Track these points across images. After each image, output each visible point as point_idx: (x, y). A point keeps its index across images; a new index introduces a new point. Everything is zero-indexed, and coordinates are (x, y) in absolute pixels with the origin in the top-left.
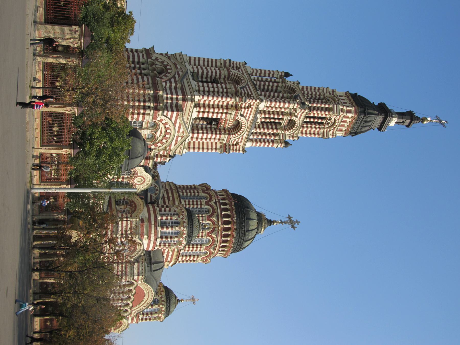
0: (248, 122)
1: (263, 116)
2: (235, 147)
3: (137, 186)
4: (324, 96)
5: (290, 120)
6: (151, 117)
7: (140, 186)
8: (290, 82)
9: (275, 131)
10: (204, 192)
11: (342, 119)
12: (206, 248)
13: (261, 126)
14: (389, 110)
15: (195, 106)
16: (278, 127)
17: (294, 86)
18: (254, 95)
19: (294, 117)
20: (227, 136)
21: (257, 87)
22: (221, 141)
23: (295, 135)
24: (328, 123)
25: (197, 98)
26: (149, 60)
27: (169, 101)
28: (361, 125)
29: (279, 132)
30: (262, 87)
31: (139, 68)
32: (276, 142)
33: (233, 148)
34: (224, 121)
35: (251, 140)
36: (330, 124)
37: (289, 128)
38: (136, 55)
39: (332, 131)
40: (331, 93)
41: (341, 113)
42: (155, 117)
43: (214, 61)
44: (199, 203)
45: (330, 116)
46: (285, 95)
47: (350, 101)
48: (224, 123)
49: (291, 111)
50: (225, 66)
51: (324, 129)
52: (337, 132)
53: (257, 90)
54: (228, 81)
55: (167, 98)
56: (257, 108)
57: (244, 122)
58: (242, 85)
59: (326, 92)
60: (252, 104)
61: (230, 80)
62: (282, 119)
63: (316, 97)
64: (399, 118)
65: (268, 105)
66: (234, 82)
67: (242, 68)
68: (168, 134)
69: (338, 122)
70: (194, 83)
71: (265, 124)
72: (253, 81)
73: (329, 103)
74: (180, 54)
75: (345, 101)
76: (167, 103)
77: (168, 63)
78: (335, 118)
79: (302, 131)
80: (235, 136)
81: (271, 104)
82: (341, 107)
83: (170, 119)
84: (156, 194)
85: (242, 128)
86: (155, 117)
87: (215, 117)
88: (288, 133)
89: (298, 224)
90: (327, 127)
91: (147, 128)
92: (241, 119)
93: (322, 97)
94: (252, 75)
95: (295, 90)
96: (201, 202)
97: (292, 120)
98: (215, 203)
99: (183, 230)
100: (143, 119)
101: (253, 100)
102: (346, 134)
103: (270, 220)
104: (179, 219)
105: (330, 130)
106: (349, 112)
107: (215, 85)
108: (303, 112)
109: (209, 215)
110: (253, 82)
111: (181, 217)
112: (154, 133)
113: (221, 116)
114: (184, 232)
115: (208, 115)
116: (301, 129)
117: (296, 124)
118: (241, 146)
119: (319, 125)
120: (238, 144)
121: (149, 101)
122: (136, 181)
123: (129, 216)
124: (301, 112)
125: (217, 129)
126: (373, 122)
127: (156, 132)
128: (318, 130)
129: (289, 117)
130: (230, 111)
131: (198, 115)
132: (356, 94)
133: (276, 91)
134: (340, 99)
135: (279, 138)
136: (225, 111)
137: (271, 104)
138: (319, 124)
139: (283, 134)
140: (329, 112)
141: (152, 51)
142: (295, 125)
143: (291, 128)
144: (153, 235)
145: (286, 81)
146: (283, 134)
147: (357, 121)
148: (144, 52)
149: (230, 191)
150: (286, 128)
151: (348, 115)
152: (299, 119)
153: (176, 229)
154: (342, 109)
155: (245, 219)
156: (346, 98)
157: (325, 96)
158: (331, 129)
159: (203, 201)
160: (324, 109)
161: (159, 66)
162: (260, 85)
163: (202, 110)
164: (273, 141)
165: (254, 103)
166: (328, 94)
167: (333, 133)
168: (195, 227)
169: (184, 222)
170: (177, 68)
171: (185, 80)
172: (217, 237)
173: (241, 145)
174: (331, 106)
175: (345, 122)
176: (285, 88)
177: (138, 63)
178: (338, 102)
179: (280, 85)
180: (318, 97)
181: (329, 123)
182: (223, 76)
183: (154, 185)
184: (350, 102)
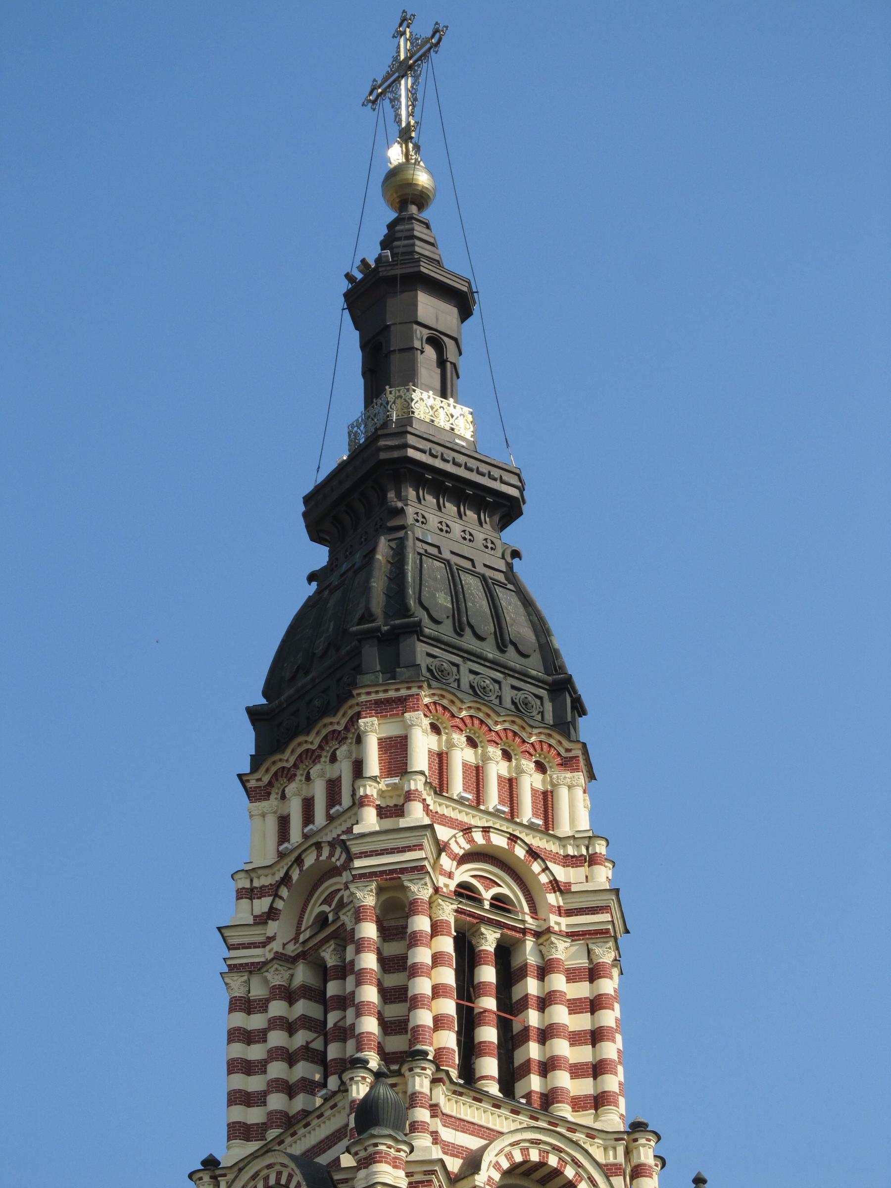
4: (293, 960)
11: (460, 801)
14: (357, 453)
23: (621, 1159)
24: (500, 903)
28: (489, 650)
36: (505, 890)
39: (561, 873)
40: (262, 905)
41: (416, 815)
45: (445, 897)
47: (312, 756)
51: (549, 930)
52: (564, 828)
59: (264, 945)
63: (306, 1022)
64: (410, 378)
69: (486, 830)
73: (346, 918)
75: (319, 791)
78: (453, 857)
79: (578, 1104)
82: (370, 820)
90: (534, 911)
93: (302, 975)
102: (567, 763)
105: (556, 886)
108: (434, 1109)
116: (564, 1111)
119: (523, 972)
124: (437, 1125)
126: (460, 568)
128: (558, 982)
134: (306, 836)
140: (410, 908)
142: (542, 1164)
147: (465, 685)
152: (492, 1135)
154: (383, 813)
156: (291, 788)
158: (544, 879)
160: (393, 949)
166: (272, 927)
167: (569, 861)
178: (332, 845)
180: (302, 1007)
181: (496, 898)
184: (325, 757)
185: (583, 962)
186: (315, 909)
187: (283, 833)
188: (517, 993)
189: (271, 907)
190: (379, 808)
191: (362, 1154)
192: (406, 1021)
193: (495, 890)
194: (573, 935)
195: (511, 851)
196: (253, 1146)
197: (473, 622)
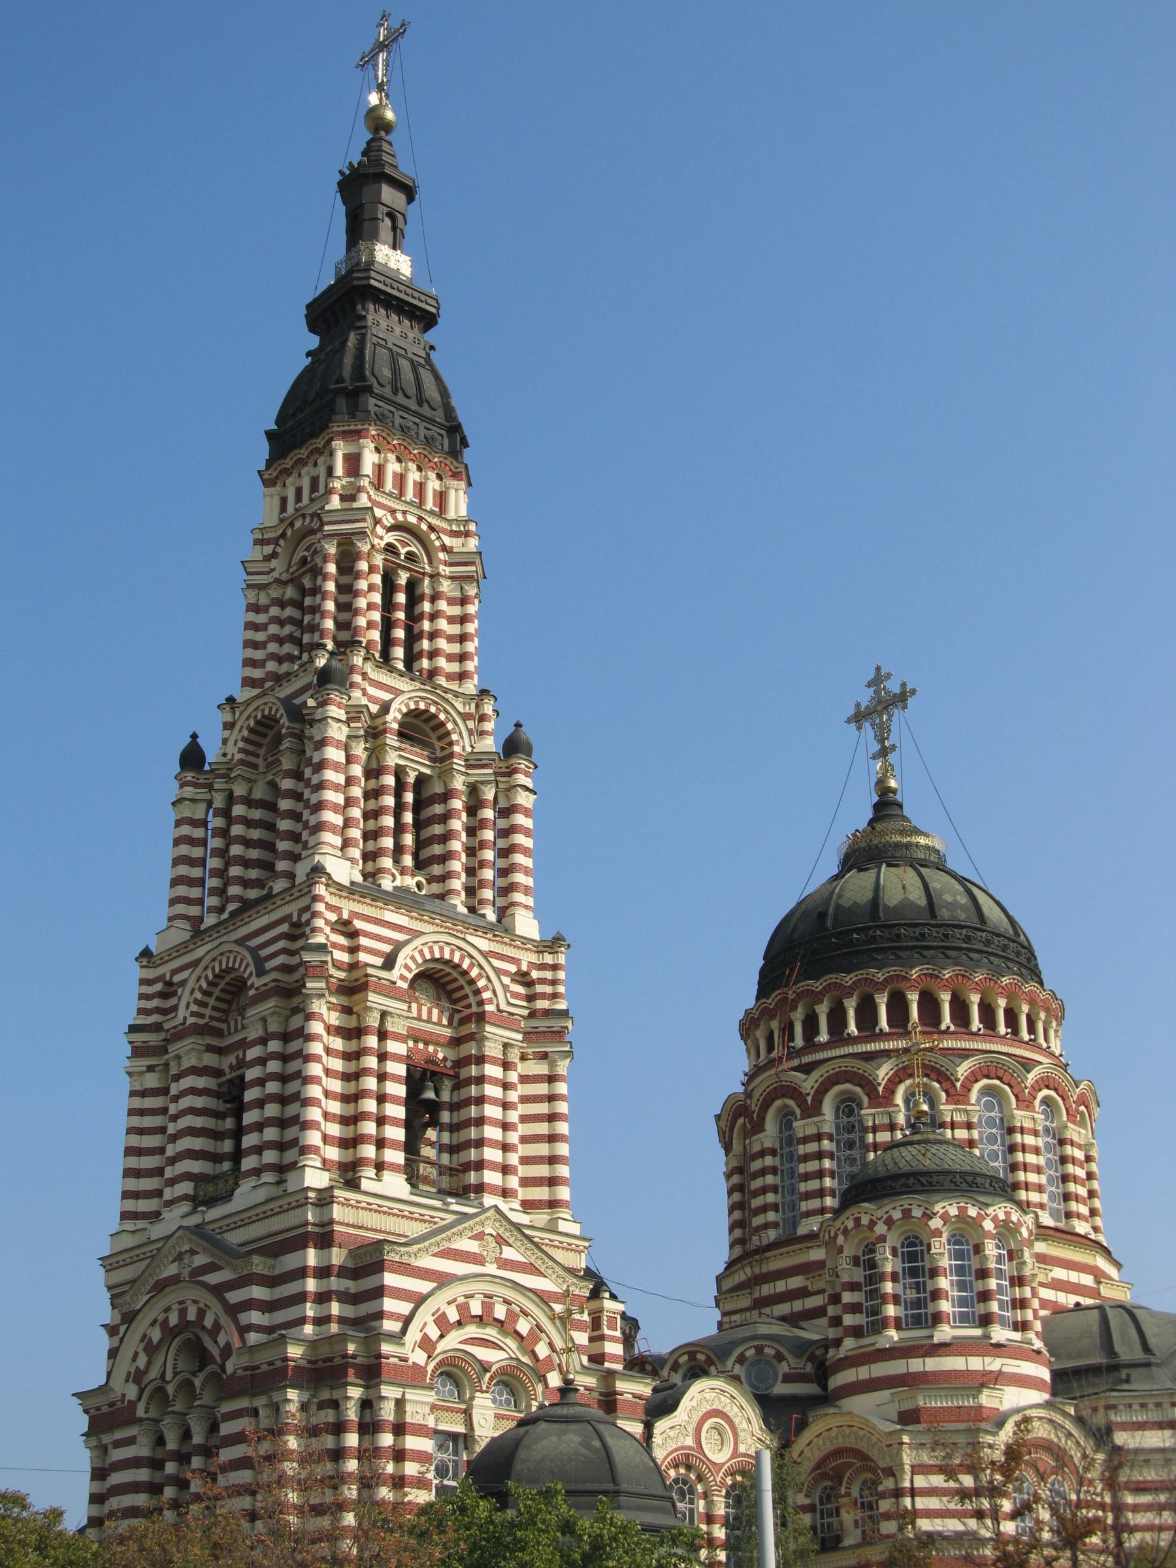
0: (418, 934)
1: (387, 862)
2: (539, 988)
3: (742, 1449)
5: (401, 735)
6: (412, 1395)
7: (742, 1435)
8: (225, 741)
9: (457, 804)
10: (758, 1127)
11: (390, 494)
12: (1025, 1103)
13: (437, 870)
14: (340, 280)
15: (352, 1184)
16: (438, 789)
17: (245, 721)
18: (292, 909)
19: (389, 718)
20: (488, 1028)
21: (253, 894)
22: (514, 1056)
23: (473, 710)
24: (411, 556)
25: (315, 1178)
26: (140, 1412)
27: (335, 1308)
28: (413, 405)
29: (459, 783)
30: (253, 874)
31: (183, 1458)
32: (508, 797)
33: (544, 996)
34: (421, 1046)
35: (502, 912)
36: (413, 549)
37: (440, 738)
38: (116, 1478)
39: (448, 541)
40: (268, 549)
41: (363, 501)
42: (413, 1377)
43: (138, 1103)
44: (812, 1147)
45: (378, 551)
46: (287, 763)
47: (302, 462)
48: (426, 1044)
49: (362, 732)
50: (162, 1050)
51: (438, 574)
52: (451, 515)
53: (269, 896)
54: (230, 1034)
55: (320, 1321)
56: (351, 890)
57: (421, 952)
58: (247, 965)
59: (268, 573)
60: (333, 917)
61: (224, 1026)
62: (399, 772)
63: (291, 620)
64: (374, 236)
65: (337, 841)
66: (234, 1006)
67: (165, 969)
68: (488, 1307)
69: (404, 513)
70: (246, 1194)
71: (425, 853)
72: (225, 916)
73: (318, 560)
74: (110, 1263)
75: (306, 483)
76: (342, 1320)
77: (153, 1324)
78: (384, 527)
79: (450, 677)
80: (486, 988)
81: (333, 829)
82: (335, 502)
83: (420, 1300)
84: (779, 1357)
85: (447, 956)
86: (413, 1377)
87: (400, 1090)
88: (462, 744)
89: (889, 676)
90: (430, 562)
91: (468, 1413)
92: (406, 967)
93: (290, 592)
94: (201, 919)
95: (264, 716)
96: (805, 1140)
97: (401, 724)
98: (807, 1069)
99: (945, 1217)
100: (421, 1430)
101: (315, 914)
102: (456, 476)
103: (877, 807)
104: (894, 1239)
105: (444, 548)
106: (353, 463)
107: (250, 1095)
108: (365, 676)
109: (865, 1100)
110: (233, 914)
111: (880, 1229)
112: (488, 1375)
113: (397, 1058)
114: (953, 1211)
115: (395, 1122)
116: (441, 681)
117: (422, 706)
118: (533, 958)
119: (421, 598)
120: (526, 974)
121: (335, 1404)
122: (719, 1454)
123: (888, 1484)
124: (365, 685)
125: (457, 1076)
126: (398, 354)
127: (485, 1367)
128: (442, 605)
129: (389, 741)
130: (373, 1021)
131: (394, 1167)
132: (270, 435)
133: (271, 807)
134: (297, 510)
135: (489, 782)
136: (372, 1041)
137: (333, 829)
138: (414, 598)
139: (468, 766)
140: (356, 556)
141: (99, 1401)
142: (426, 711)
143: (441, 731)
144: (976, 1363)
145: (223, 759)
146: (468, 766)
148: (107, 1439)
149: (750, 1001)
150: (439, 754)
151: (367, 468)
152: (398, 692)
153: (942, 1253)
154: (343, 498)
155: (878, 927)
156: (289, 481)
157: (285, 577)
158: (437, 543)
159: (803, 1127)
160: (345, 580)
161: (169, 1363)
162: (245, 883)
163: (369, 1151)
164: (506, 812)
165: (329, 907)
166: (274, 563)
168: (928, 1164)
169: (907, 1213)
170: (175, 1280)
171: (234, 1238)
172: (966, 1057)
173: (527, 958)
174: (332, 549)
175: (401, 480)
176: (255, 766)
177: (156, 1464)
178: (312, 516)
179: (239, 790)
180: (289, 612)
181: (408, 553)
182: (210, 1060)
183: (737, 1366)
185: (458, 594)
186: (300, 554)
187: (283, 508)
188: (417, 611)
189: (274, 551)
190: (341, 495)
191: (320, 699)
192: (351, 623)
193: (408, 549)
194: (452, 578)
195: (418, 526)
196: (256, 691)
197: (404, 387)
